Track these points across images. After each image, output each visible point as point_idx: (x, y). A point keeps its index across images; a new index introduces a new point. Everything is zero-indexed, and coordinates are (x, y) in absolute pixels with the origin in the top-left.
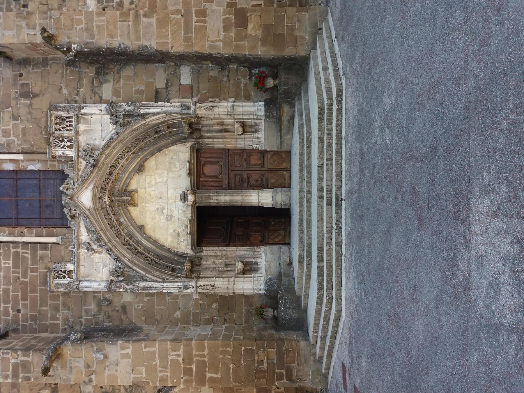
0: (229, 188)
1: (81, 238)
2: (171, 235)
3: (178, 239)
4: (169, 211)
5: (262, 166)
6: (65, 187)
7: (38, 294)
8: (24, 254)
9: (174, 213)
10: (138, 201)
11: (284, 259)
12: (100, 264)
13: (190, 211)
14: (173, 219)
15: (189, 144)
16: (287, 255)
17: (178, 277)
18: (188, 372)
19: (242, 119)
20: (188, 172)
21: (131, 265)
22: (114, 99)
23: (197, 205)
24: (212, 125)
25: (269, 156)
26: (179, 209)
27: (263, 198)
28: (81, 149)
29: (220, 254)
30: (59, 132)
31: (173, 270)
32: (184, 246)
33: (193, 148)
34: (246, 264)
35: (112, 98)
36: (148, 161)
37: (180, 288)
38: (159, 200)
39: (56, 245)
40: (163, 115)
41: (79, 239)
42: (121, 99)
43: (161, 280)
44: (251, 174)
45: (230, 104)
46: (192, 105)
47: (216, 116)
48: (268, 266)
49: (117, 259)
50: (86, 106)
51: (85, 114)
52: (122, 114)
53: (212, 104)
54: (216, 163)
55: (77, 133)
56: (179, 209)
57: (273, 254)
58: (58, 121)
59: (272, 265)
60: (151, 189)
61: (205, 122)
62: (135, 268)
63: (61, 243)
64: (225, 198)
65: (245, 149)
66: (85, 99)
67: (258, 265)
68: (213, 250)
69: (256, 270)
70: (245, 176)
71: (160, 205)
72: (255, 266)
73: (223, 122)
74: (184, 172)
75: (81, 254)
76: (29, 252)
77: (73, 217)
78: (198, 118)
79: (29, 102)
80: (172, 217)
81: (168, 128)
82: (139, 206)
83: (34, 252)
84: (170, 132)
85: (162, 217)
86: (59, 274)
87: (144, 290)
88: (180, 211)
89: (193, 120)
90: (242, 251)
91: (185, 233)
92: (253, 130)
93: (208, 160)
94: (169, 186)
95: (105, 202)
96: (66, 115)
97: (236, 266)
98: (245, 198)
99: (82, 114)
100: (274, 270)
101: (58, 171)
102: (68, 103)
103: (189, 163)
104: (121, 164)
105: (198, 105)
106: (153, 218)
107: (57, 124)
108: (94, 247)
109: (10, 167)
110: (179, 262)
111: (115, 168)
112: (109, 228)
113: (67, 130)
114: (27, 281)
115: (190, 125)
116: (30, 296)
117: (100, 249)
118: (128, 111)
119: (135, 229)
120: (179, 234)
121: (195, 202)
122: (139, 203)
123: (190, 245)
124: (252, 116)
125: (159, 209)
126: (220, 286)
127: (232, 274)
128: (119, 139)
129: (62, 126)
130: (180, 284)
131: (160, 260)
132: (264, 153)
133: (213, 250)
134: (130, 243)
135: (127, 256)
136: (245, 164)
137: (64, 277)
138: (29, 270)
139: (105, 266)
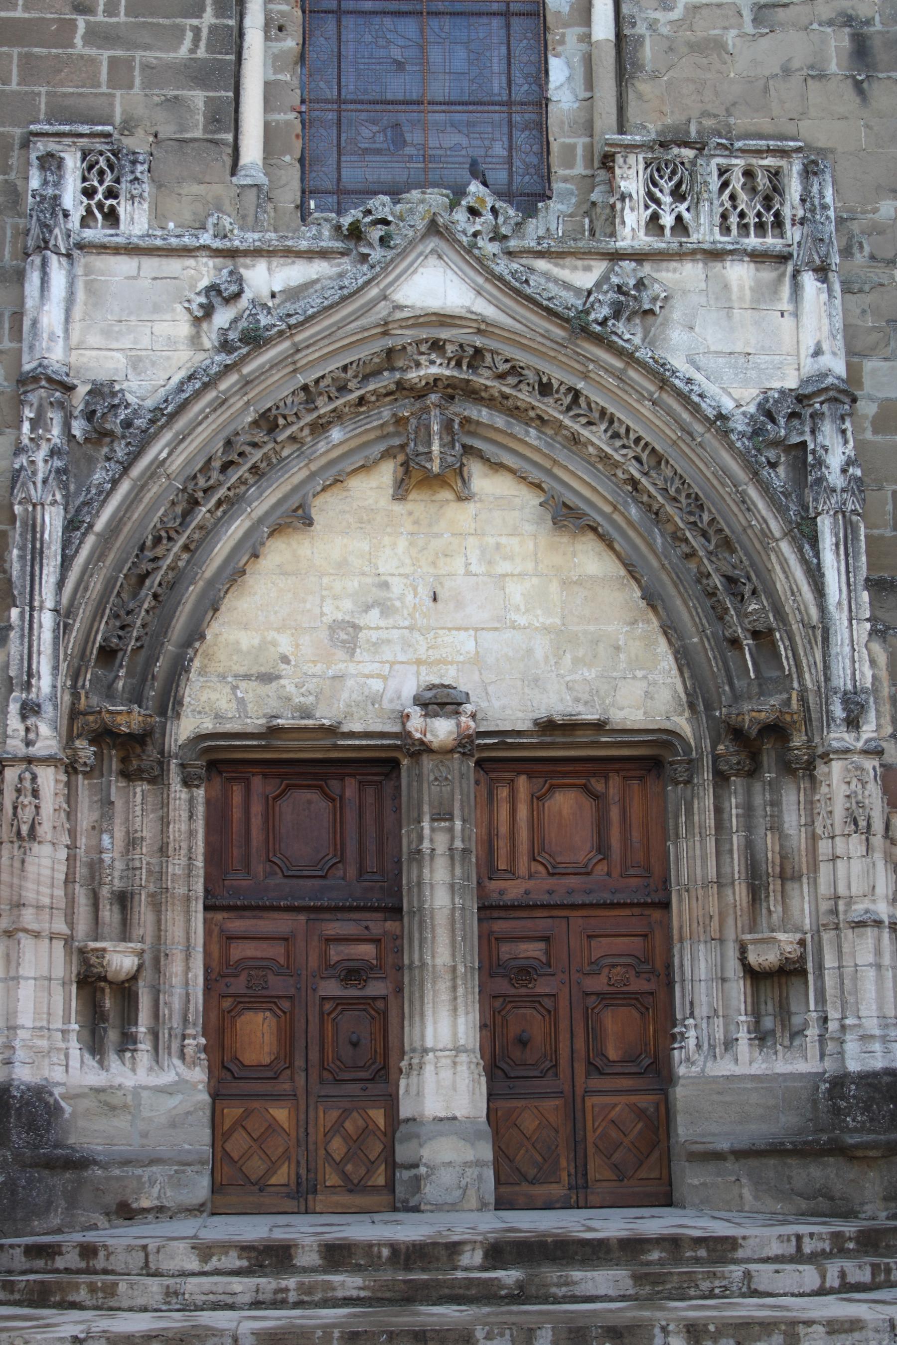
0: (488, 910)
1: (261, 266)
2: (264, 645)
3: (247, 677)
4: (374, 636)
5: (593, 1069)
6: (483, 201)
7: (14, 86)
8: (189, 35)
9: (366, 656)
10: (418, 504)
11: (152, 1183)
12: (145, 342)
13: (378, 728)
14: (340, 654)
15: (683, 724)
16: (172, 1198)
17: (76, 675)
19: (820, 967)
20: (557, 718)
21: (136, 471)
22: (867, 408)
23: (405, 762)
24: (776, 827)
25: (645, 1101)
26: (385, 678)
27: (446, 1074)
28: (647, 269)
29: (176, 867)
30: (715, 182)
31: (108, 654)
33: (667, 745)
34: (126, 991)
35: (871, 399)
36: (600, 546)
37: (28, 686)
38: (424, 594)
39: (228, 161)
40: (814, 612)
41: (257, 253)
42: (869, 435)
43: (65, 601)
44: (552, 1014)
45: (883, 910)
46: (865, 736)
47: (824, 847)
48: (115, 1101)
50: (830, 290)
51: (796, 288)
52: (808, 437)
53: (878, 826)
54: (602, 848)
55: (715, 255)
56: (385, 678)
57: (173, 1125)
58: (762, 181)
59: (121, 1122)
60: (473, 560)
61: (790, 798)
62: (125, 487)
63: (234, 179)
65: (670, 985)
66: (860, 291)
67: (121, 1051)
68: (191, 833)
69: (95, 1046)
70: (542, 987)
71: (401, 598)
72: (113, 1036)
73: (797, 878)
74: (556, 702)
75: (191, 262)
76: (201, 53)
78: (810, 767)
79: (833, 68)
80: (351, 647)
81: (756, 634)
82: (398, 508)
83: (199, 74)
84: (735, 643)
85: (347, 604)
86: (101, 173)
87: (25, 524)
88: (376, 685)
89: (798, 740)
90: (186, 979)
91: (273, 705)
92: (768, 1023)
93: (615, 814)
94: (489, 635)
95: (418, 365)
96: (787, 213)
97: (122, 946)
98: (443, 986)
99: (796, 274)
100: (89, 1133)
101: (547, 177)
102: (840, 221)
103: (599, 726)
104: (585, 433)
105: (870, 764)
106: (342, 567)
107: (748, 174)
108: (222, 317)
110: (144, 681)
111: (569, 409)
112: (301, 379)
113: (724, 216)
114: (73, 46)
115: (777, 731)
116: (10, 56)
117: (210, 340)
118: (820, 463)
119: (295, 489)
120: (267, 678)
121: (425, 748)
122: (410, 506)
123: (221, 729)
124: (834, 1014)
125: (383, 594)
126: (31, 868)
127: (82, 927)
128: (698, 428)
129: (743, 197)
130: (45, 683)
131: (155, 596)
132: (657, 1071)
133: (191, 833)
134: (234, 467)
135: (174, 455)
136: (598, 984)
137: (89, 193)
138: (119, 53)
139: (136, 363)
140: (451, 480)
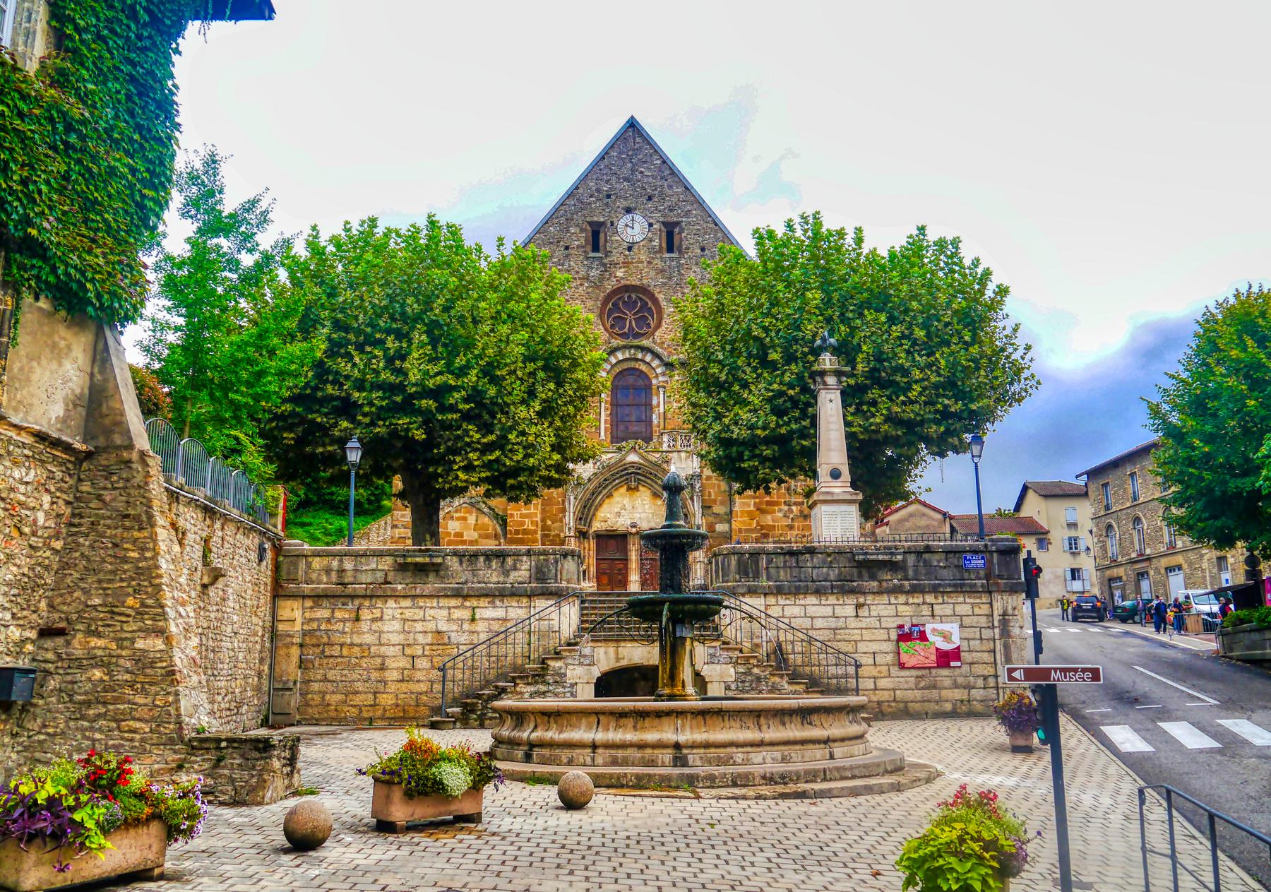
18: (517, 532)
32: (597, 526)
49: (589, 480)
64: (634, 556)
77: (620, 449)
90: (593, 570)
109: (654, 402)
134: (601, 487)
140: (636, 489)
